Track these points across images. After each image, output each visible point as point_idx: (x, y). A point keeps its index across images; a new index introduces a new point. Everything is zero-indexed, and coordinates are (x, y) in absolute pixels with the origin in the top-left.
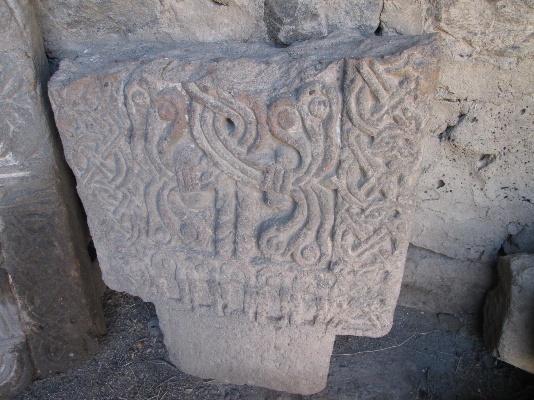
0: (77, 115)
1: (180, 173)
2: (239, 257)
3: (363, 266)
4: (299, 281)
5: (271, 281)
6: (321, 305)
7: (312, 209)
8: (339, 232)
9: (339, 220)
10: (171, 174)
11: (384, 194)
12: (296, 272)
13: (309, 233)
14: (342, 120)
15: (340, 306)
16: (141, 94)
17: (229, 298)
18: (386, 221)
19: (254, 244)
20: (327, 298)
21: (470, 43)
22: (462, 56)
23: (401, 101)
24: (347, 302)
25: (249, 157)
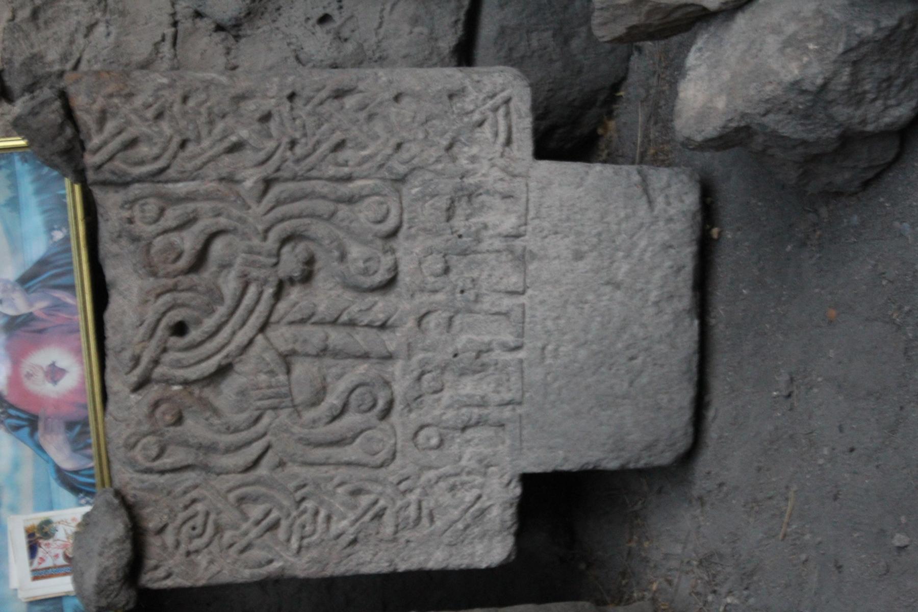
0: (183, 548)
1: (259, 403)
2: (395, 320)
3: (390, 131)
4: (429, 225)
5: (439, 266)
6: (473, 188)
7: (296, 212)
8: (332, 171)
9: (314, 173)
10: (265, 420)
11: (266, 118)
12: (413, 231)
13: (340, 214)
14: (167, 182)
15: (473, 159)
16: (144, 448)
17: (487, 338)
18: (309, 107)
19: (377, 299)
20: (458, 180)
21: (91, 28)
22: (108, 34)
23: (135, 111)
24: (466, 149)
25: (229, 301)
